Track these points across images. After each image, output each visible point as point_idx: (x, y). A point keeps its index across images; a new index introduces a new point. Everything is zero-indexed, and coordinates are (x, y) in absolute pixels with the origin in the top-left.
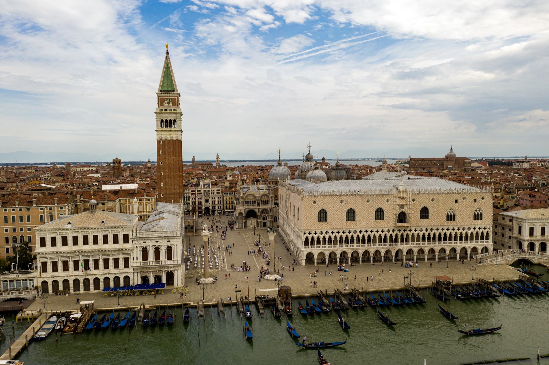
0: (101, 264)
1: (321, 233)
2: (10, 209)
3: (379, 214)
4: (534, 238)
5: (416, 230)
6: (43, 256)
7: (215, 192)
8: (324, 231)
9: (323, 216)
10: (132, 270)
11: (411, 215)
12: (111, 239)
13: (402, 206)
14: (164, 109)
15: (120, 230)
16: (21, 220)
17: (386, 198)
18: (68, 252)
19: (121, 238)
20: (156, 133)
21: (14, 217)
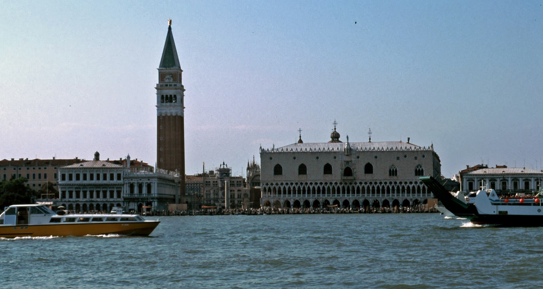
0: (101, 194)
1: (277, 184)
6: (64, 187)
8: (279, 183)
9: (278, 170)
10: (123, 200)
11: (355, 170)
12: (108, 176)
13: (348, 162)
14: (164, 84)
15: (115, 170)
16: (40, 177)
18: (80, 185)
19: (115, 176)
20: (156, 108)
21: (34, 175)
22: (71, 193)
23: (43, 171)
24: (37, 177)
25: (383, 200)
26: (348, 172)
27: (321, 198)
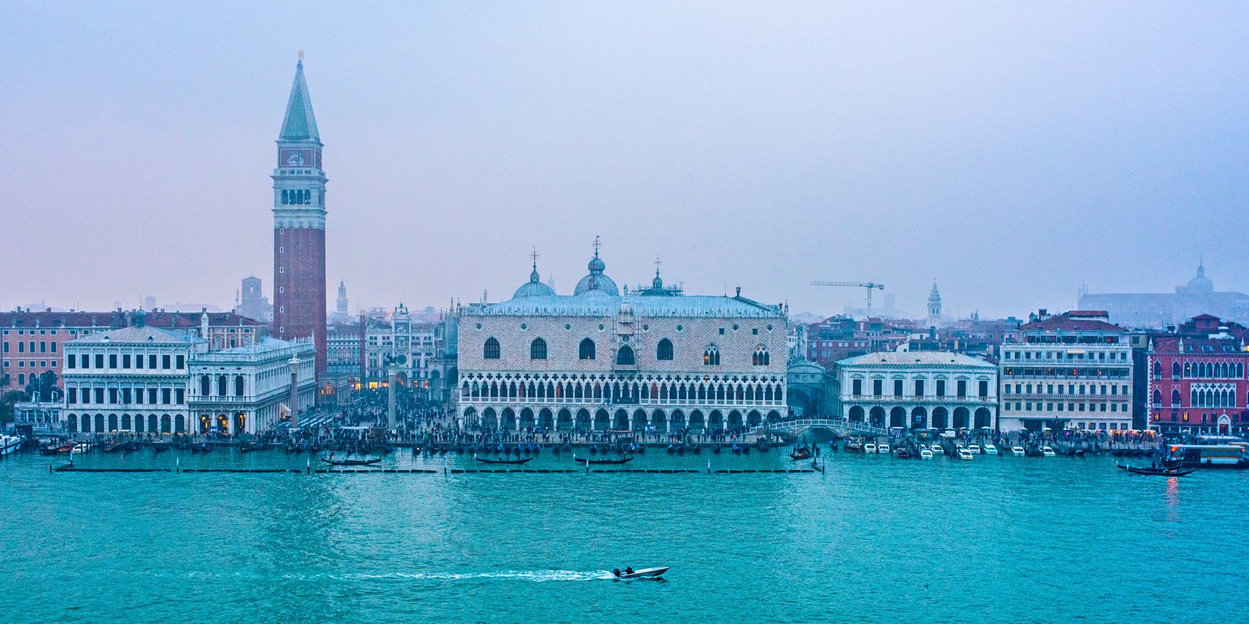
0: (146, 395)
1: (490, 377)
2: (27, 331)
3: (587, 349)
4: (862, 398)
5: (650, 378)
7: (422, 341)
8: (494, 374)
9: (492, 349)
11: (640, 353)
12: (159, 361)
13: (626, 337)
16: (43, 350)
17: (596, 323)
19: (173, 361)
21: (32, 344)
22: (86, 392)
23: (49, 338)
24: (38, 348)
25: (691, 410)
26: (626, 355)
27: (574, 405)
